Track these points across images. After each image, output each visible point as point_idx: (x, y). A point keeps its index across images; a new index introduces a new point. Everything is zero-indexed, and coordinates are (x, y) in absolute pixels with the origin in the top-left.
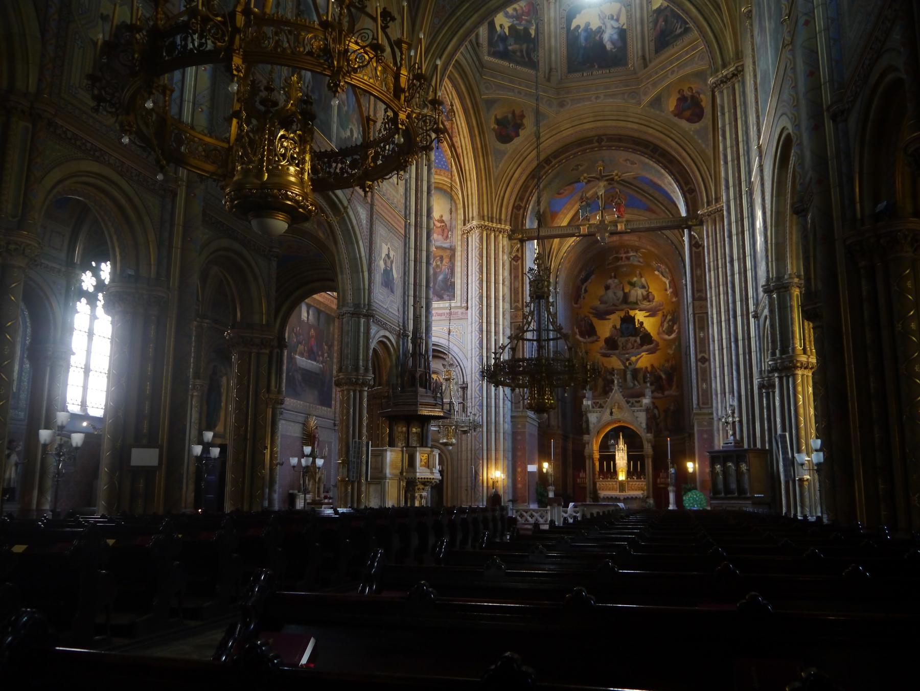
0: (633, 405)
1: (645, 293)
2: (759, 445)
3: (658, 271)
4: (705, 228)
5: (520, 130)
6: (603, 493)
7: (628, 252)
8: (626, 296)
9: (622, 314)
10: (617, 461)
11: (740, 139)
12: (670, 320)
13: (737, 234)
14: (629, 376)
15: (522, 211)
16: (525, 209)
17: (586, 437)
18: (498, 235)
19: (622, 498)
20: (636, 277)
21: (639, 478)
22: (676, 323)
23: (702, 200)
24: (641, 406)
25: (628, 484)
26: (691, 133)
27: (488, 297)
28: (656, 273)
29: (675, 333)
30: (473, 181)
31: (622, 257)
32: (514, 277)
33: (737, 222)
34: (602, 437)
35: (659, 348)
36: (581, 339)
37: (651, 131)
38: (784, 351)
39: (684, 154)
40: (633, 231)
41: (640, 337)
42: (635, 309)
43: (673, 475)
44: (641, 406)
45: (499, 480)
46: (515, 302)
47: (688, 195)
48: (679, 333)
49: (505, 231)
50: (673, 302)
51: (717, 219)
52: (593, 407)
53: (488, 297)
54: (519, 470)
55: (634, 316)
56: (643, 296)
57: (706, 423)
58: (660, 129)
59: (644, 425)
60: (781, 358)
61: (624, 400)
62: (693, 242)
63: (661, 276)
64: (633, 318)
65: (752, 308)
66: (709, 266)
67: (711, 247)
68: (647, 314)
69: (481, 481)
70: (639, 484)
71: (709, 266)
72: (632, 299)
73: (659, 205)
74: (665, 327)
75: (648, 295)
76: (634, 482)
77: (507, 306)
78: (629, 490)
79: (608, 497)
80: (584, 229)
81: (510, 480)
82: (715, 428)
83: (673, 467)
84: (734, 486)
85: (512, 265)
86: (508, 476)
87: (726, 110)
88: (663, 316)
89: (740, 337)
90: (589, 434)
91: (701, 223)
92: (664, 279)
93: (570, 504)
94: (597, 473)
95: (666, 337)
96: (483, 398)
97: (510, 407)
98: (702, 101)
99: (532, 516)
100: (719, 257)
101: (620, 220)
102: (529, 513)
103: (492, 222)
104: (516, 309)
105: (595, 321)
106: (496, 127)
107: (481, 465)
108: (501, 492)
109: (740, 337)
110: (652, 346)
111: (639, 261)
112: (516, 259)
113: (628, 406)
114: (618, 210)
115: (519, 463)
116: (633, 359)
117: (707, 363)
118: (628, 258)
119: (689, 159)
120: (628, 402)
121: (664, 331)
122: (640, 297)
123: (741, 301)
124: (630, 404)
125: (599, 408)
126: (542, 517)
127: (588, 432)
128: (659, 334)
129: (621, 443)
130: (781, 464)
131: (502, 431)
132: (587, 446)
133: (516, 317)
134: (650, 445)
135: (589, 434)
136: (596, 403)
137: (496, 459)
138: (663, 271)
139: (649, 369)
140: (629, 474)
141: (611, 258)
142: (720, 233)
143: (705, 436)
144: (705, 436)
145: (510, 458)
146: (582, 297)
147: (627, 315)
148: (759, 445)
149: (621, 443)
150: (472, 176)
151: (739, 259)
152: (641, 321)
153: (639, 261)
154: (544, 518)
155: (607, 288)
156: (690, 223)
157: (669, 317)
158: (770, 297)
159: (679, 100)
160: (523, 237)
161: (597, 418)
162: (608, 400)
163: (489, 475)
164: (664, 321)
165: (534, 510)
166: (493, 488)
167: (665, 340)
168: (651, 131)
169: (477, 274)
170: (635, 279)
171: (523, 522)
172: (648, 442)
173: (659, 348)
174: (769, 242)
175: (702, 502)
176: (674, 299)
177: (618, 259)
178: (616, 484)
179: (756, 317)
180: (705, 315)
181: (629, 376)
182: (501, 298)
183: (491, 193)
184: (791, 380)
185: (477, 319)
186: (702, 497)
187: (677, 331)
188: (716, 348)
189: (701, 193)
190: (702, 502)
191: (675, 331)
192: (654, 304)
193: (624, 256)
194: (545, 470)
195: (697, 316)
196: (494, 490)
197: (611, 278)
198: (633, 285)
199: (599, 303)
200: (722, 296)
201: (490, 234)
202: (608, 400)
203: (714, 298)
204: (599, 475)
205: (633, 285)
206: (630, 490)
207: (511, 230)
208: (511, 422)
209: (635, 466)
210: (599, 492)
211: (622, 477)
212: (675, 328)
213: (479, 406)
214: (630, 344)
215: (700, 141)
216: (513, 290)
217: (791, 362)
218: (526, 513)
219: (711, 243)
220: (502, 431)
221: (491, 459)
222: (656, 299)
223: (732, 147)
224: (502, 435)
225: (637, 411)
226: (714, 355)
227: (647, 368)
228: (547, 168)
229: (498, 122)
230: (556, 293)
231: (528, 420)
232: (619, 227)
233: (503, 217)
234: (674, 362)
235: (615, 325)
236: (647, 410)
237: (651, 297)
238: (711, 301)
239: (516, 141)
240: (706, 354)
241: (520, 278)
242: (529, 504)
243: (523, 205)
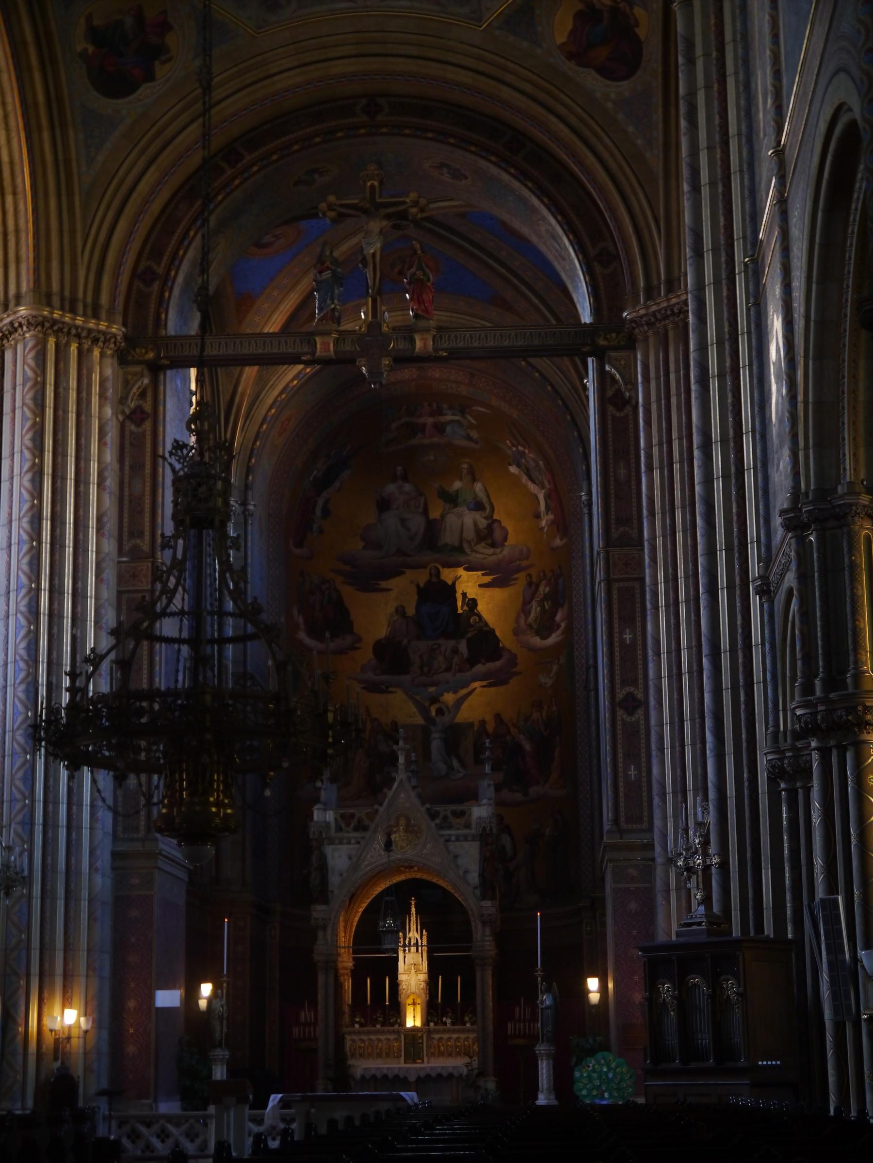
0: (445, 824)
1: (483, 523)
2: (769, 930)
3: (519, 466)
4: (639, 356)
5: (157, 63)
6: (361, 1066)
7: (440, 412)
8: (433, 528)
9: (422, 578)
11: (732, 129)
12: (546, 597)
13: (721, 376)
14: (436, 745)
15: (156, 285)
16: (167, 281)
17: (319, 911)
18: (90, 350)
19: (412, 1078)
20: (461, 479)
21: (458, 1021)
23: (634, 283)
24: (468, 826)
25: (429, 1038)
26: (610, 105)
27: (57, 519)
28: (513, 469)
29: (559, 632)
30: (20, 196)
31: (424, 425)
32: (131, 467)
33: (720, 343)
34: (361, 910)
35: (517, 669)
36: (308, 641)
37: (505, 92)
38: (833, 682)
39: (591, 159)
40: (455, 355)
41: (469, 641)
42: (457, 565)
43: (549, 1012)
44: (468, 826)
45: (75, 1033)
46: (132, 535)
47: (598, 268)
48: (569, 630)
49: (105, 338)
51: (671, 334)
52: (339, 829)
53: (57, 519)
54: (132, 1004)
55: (454, 584)
56: (477, 531)
57: (633, 872)
58: (528, 88)
59: (474, 877)
60: (825, 700)
61: (423, 809)
62: (610, 393)
63: (524, 479)
64: (452, 589)
65: (754, 569)
66: (649, 456)
67: (654, 407)
68: (488, 579)
69: (20, 1039)
70: (458, 1039)
71: (649, 456)
72: (449, 538)
73: (523, 288)
74: (533, 614)
75: (490, 528)
76: (444, 1031)
77: (110, 546)
78: (431, 1055)
79: (374, 1077)
80: (325, 345)
81: (105, 1034)
82: (659, 884)
83: (548, 990)
84: (705, 1039)
85: (127, 433)
86: (98, 1024)
87: (699, 51)
88: (530, 584)
89: (725, 642)
90: (326, 902)
91: (631, 344)
92: (533, 488)
93: (273, 1096)
94: (346, 1009)
95: (537, 641)
96: (33, 801)
97: (110, 830)
98: (637, 25)
99: (163, 1135)
100: (675, 435)
101: (423, 324)
102: (156, 1127)
103: (73, 311)
104: (135, 554)
105: (348, 592)
106: (91, 49)
107: (22, 992)
108: (78, 1070)
109: (725, 642)
110: (498, 664)
111: (469, 438)
112: (137, 416)
113: (433, 824)
114: (418, 299)
115: (132, 985)
116: (449, 698)
117: (640, 712)
118: (440, 428)
119: (602, 174)
120: (433, 816)
121: (530, 626)
122: (470, 534)
123: (729, 549)
124: (438, 821)
125: (356, 829)
126: (191, 1136)
127: (324, 896)
128: (516, 632)
130: (825, 977)
131: (85, 894)
132: (320, 934)
133: (134, 576)
136: (346, 818)
137: (67, 976)
138: (532, 464)
139: (490, 728)
140: (432, 1011)
141: (394, 426)
142: (677, 371)
143: (633, 906)
144: (633, 906)
145: (107, 972)
146: (315, 527)
147: (434, 579)
148: (769, 930)
150: (19, 181)
151: (724, 441)
152: (470, 596)
153: (469, 438)
154: (198, 1141)
155: (384, 505)
156: (602, 342)
157: (544, 589)
158: (802, 541)
159: (579, 16)
160: (158, 357)
161: (350, 858)
162: (381, 809)
163: (47, 1022)
164: (531, 600)
165: (169, 1118)
166: (56, 1059)
167: (532, 649)
168: (505, 92)
169: (27, 454)
170: (457, 485)
171: (139, 1153)
173: (517, 669)
174: (800, 398)
175: (623, 1085)
176: (558, 542)
178: (398, 1040)
179: (765, 591)
180: (637, 585)
181: (436, 745)
182: (92, 523)
183: (73, 232)
184: (849, 756)
185: (24, 579)
186: (625, 1069)
187: (563, 625)
188: (664, 672)
189: (631, 263)
190: (623, 1085)
191: (559, 626)
192: (506, 552)
193: (430, 421)
194: (203, 1004)
195: (616, 586)
196: (58, 1064)
198: (451, 500)
199: (361, 544)
200: (679, 536)
201: (68, 345)
202: (381, 809)
203: (659, 542)
204: (353, 1016)
205: (451, 500)
206: (433, 1054)
207: (126, 337)
208: (113, 869)
209: (450, 988)
210: (351, 1062)
211: (413, 1019)
212: (558, 617)
213: (22, 823)
214: (441, 658)
215: (631, 129)
216: (126, 502)
217: (851, 710)
218: (148, 1125)
219: (653, 398)
220: (85, 894)
221: (52, 975)
222: (511, 540)
223: (710, 148)
224: (84, 905)
225: (457, 840)
226: (659, 690)
227: (483, 723)
228: (229, 172)
229: (95, 35)
230: (246, 514)
231: (160, 864)
232: (419, 344)
233: (104, 300)
235: (403, 607)
236: (484, 837)
237: (498, 534)
238: (653, 549)
239: (145, 91)
240: (637, 686)
241: (148, 470)
242: (156, 1100)
243: (160, 270)
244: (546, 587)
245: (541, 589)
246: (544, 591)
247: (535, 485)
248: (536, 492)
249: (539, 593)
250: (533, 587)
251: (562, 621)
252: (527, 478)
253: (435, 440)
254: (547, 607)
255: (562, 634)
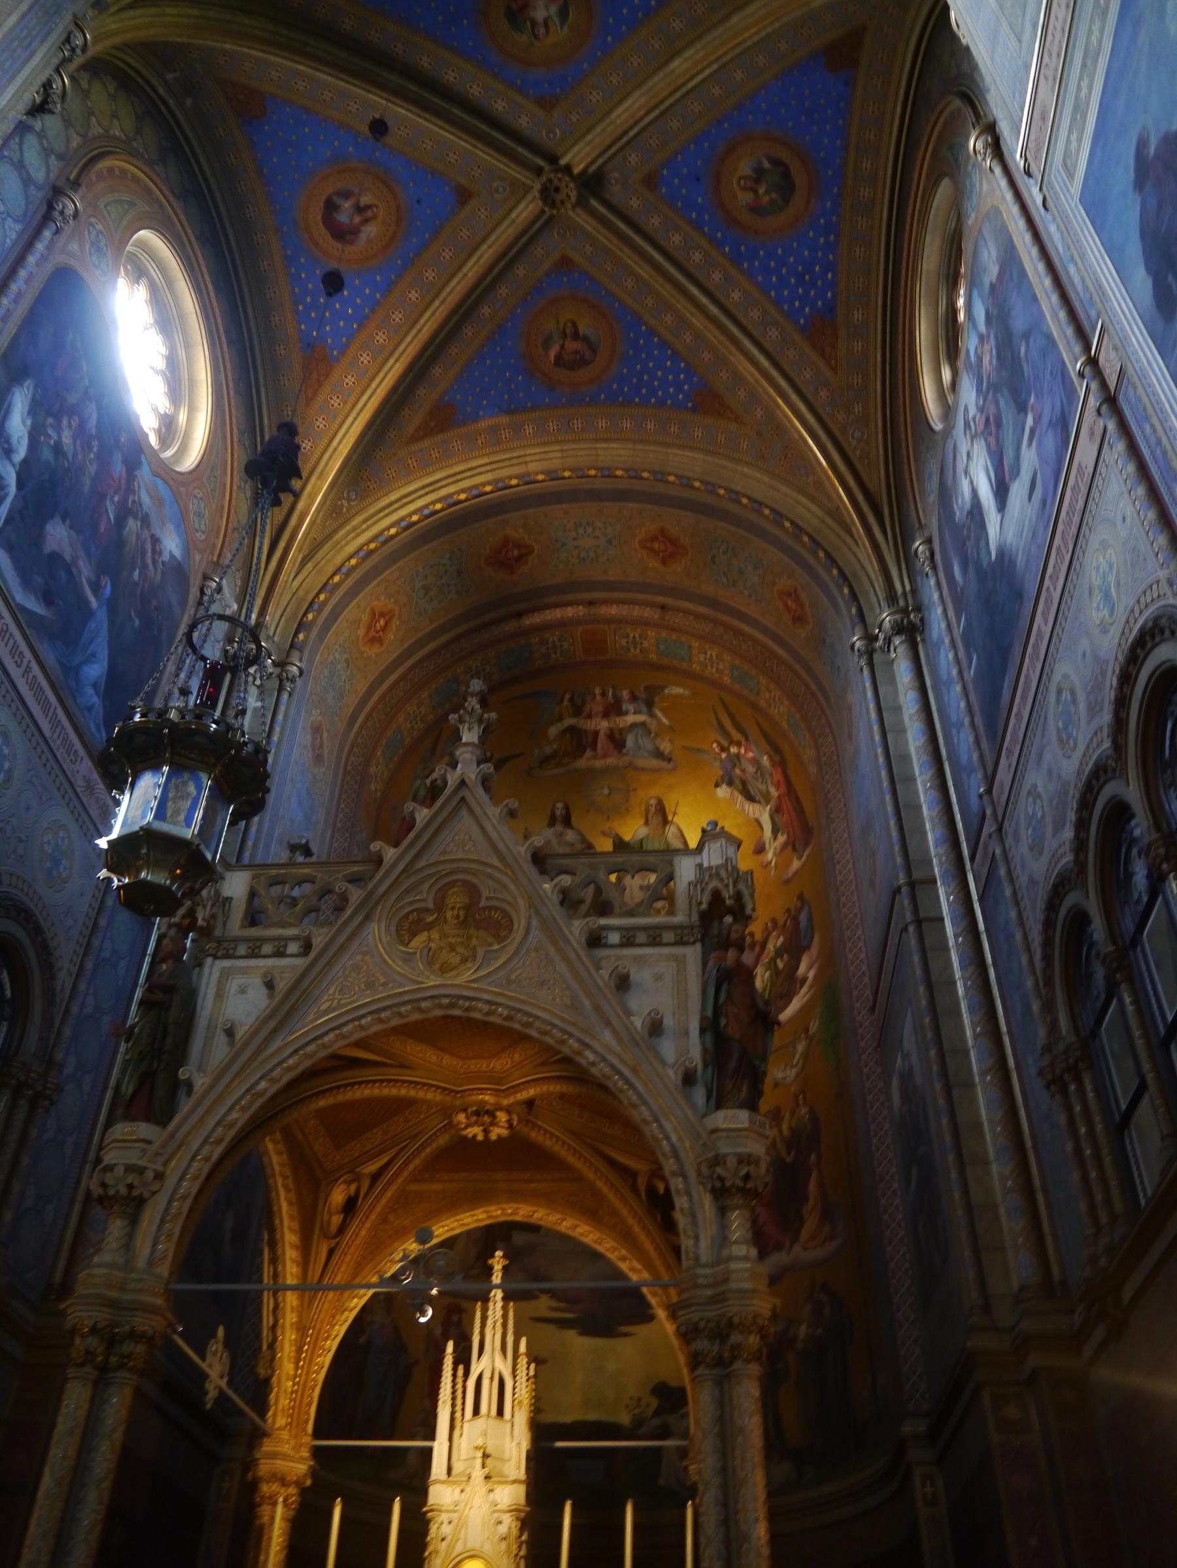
7: (614, 709)
10: (441, 1494)
12: (779, 953)
22: (807, 948)
50: (787, 882)
92: (752, 809)
118: (617, 741)
129: (493, 1338)
134: (738, 1223)
135: (161, 1115)
149: (493, 1338)
172: (720, 1193)
177: (580, 741)
187: (811, 974)
191: (804, 980)
197: (552, 822)
234: (803, 1110)
244: (778, 938)
245: (771, 947)
246: (775, 946)
247: (755, 805)
248: (757, 815)
249: (766, 952)
250: (757, 948)
251: (810, 968)
252: (743, 799)
253: (610, 761)
254: (780, 965)
255: (811, 987)
